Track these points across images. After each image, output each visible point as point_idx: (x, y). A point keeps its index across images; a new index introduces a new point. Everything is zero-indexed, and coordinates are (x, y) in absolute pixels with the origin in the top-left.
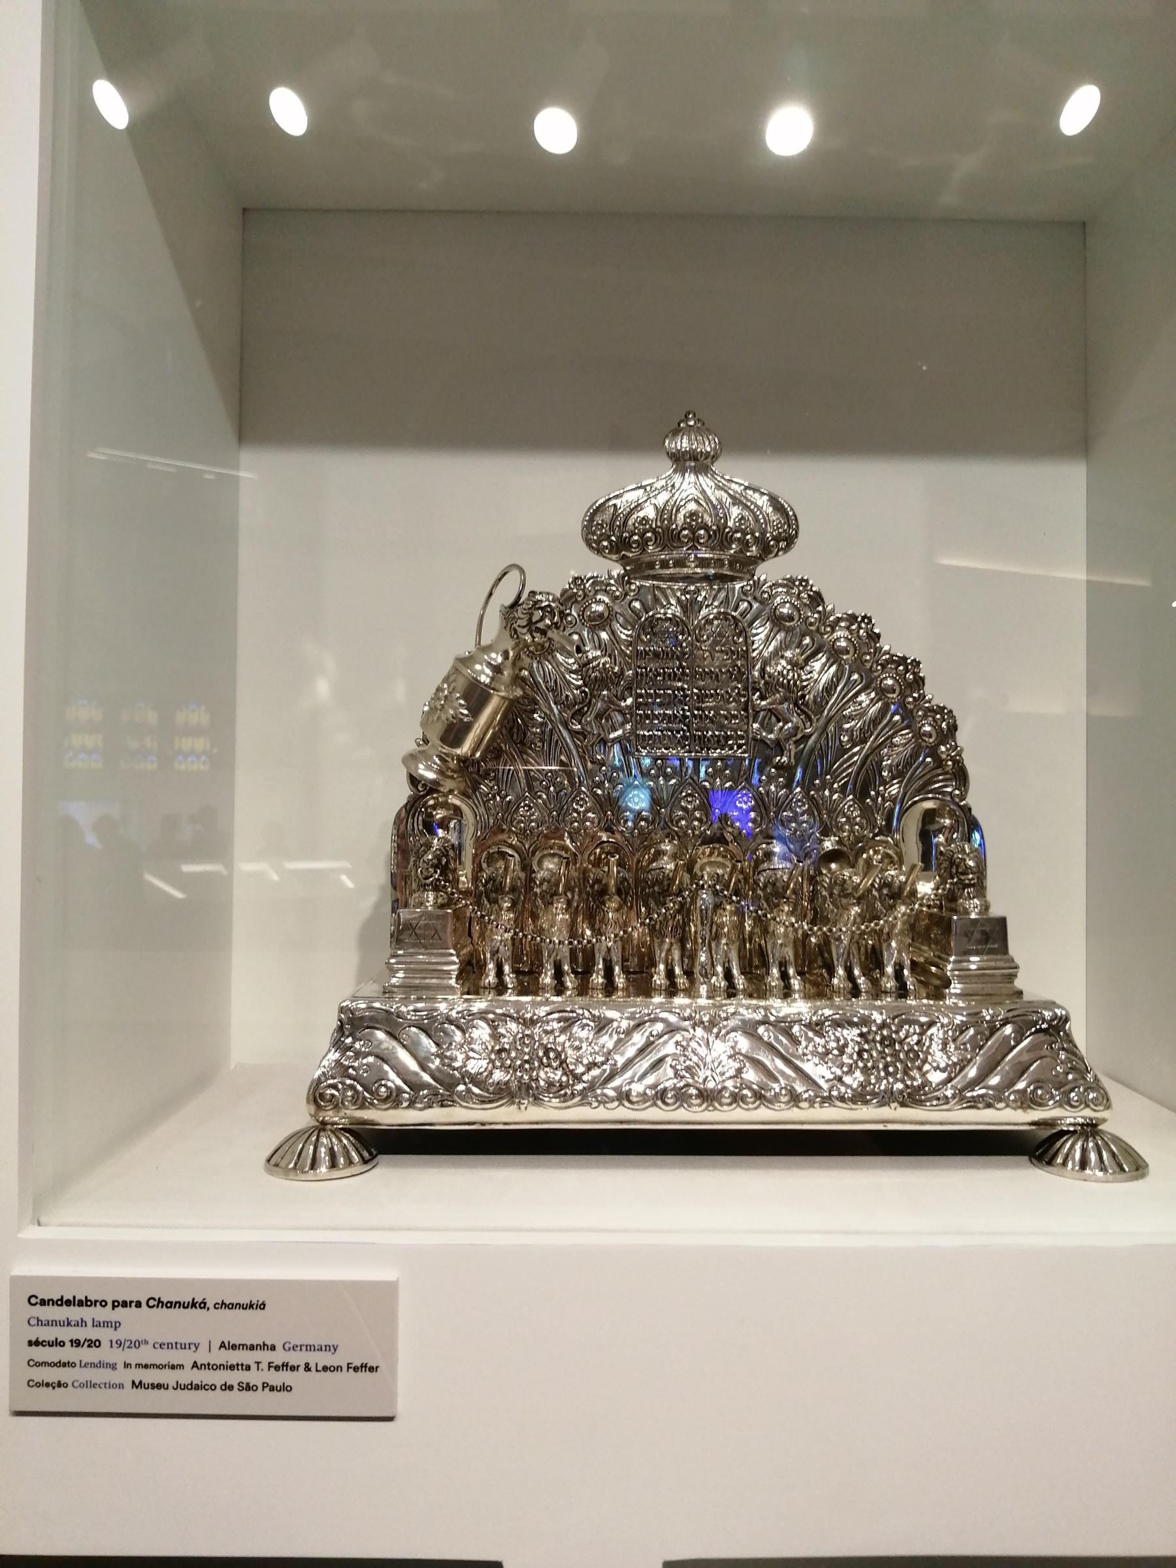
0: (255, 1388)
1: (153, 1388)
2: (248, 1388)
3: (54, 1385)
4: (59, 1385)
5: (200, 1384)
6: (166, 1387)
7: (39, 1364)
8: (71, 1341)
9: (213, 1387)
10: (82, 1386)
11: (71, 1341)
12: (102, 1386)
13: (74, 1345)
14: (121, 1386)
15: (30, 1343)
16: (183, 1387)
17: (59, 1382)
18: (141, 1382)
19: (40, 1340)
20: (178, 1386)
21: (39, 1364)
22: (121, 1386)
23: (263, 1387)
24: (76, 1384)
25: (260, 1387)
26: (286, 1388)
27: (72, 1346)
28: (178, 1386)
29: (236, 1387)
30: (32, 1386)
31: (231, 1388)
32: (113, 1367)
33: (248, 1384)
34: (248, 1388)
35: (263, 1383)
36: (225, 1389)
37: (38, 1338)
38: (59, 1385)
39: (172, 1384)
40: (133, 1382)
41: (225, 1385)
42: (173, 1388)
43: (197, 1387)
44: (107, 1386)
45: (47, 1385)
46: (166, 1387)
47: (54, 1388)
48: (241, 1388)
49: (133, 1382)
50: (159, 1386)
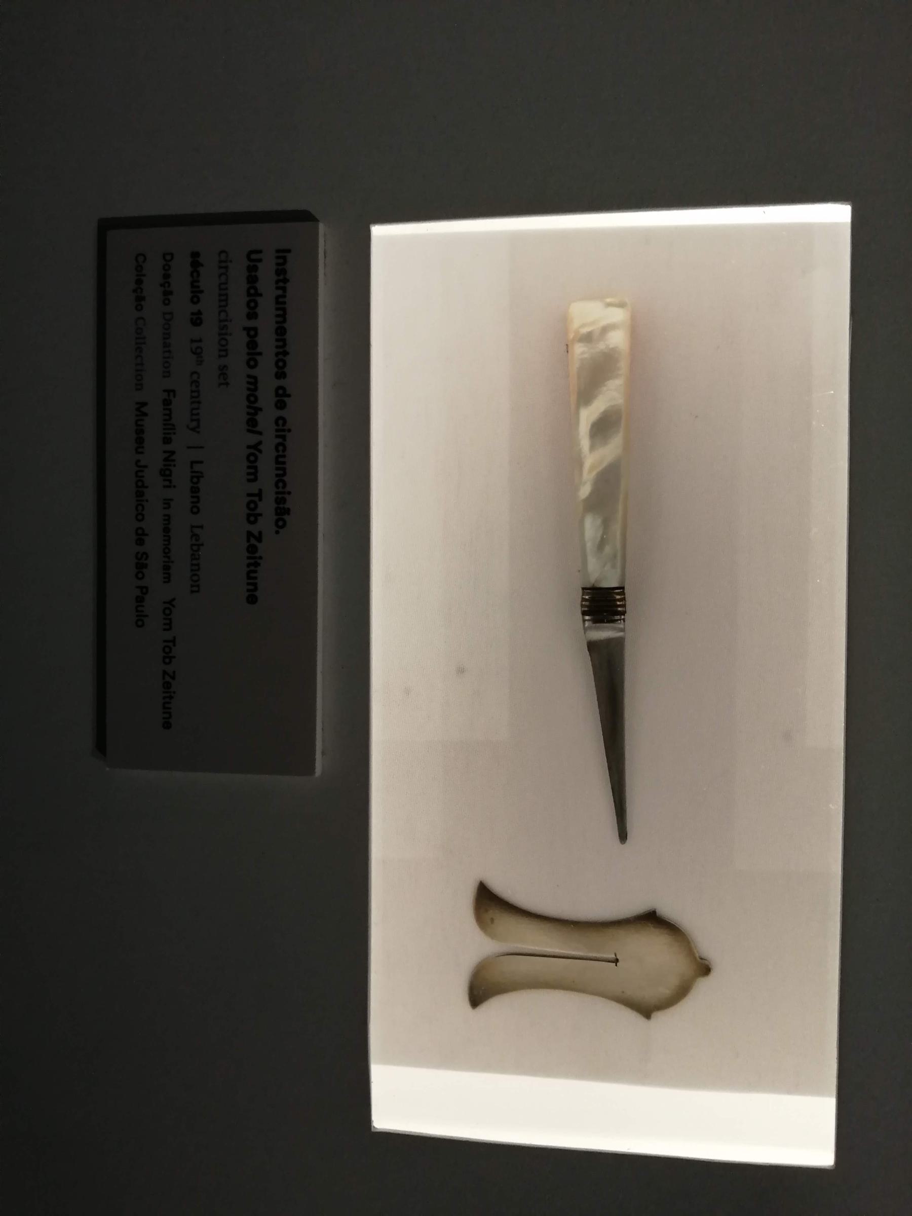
2: (141, 567)
3: (139, 290)
4: (140, 299)
6: (140, 450)
7: (167, 268)
8: (200, 313)
9: (140, 517)
11: (200, 313)
13: (194, 317)
15: (195, 255)
16: (140, 474)
17: (143, 299)
18: (146, 414)
19: (201, 269)
20: (140, 468)
21: (167, 268)
22: (139, 387)
23: (141, 588)
26: (140, 621)
27: (193, 314)
28: (140, 468)
30: (137, 260)
31: (140, 542)
32: (167, 374)
33: (146, 566)
34: (141, 567)
35: (146, 588)
36: (137, 534)
37: (202, 265)
40: (144, 404)
41: (144, 534)
43: (140, 494)
45: (139, 282)
46: (140, 450)
47: (135, 291)
48: (139, 556)
49: (144, 404)
50: (140, 441)
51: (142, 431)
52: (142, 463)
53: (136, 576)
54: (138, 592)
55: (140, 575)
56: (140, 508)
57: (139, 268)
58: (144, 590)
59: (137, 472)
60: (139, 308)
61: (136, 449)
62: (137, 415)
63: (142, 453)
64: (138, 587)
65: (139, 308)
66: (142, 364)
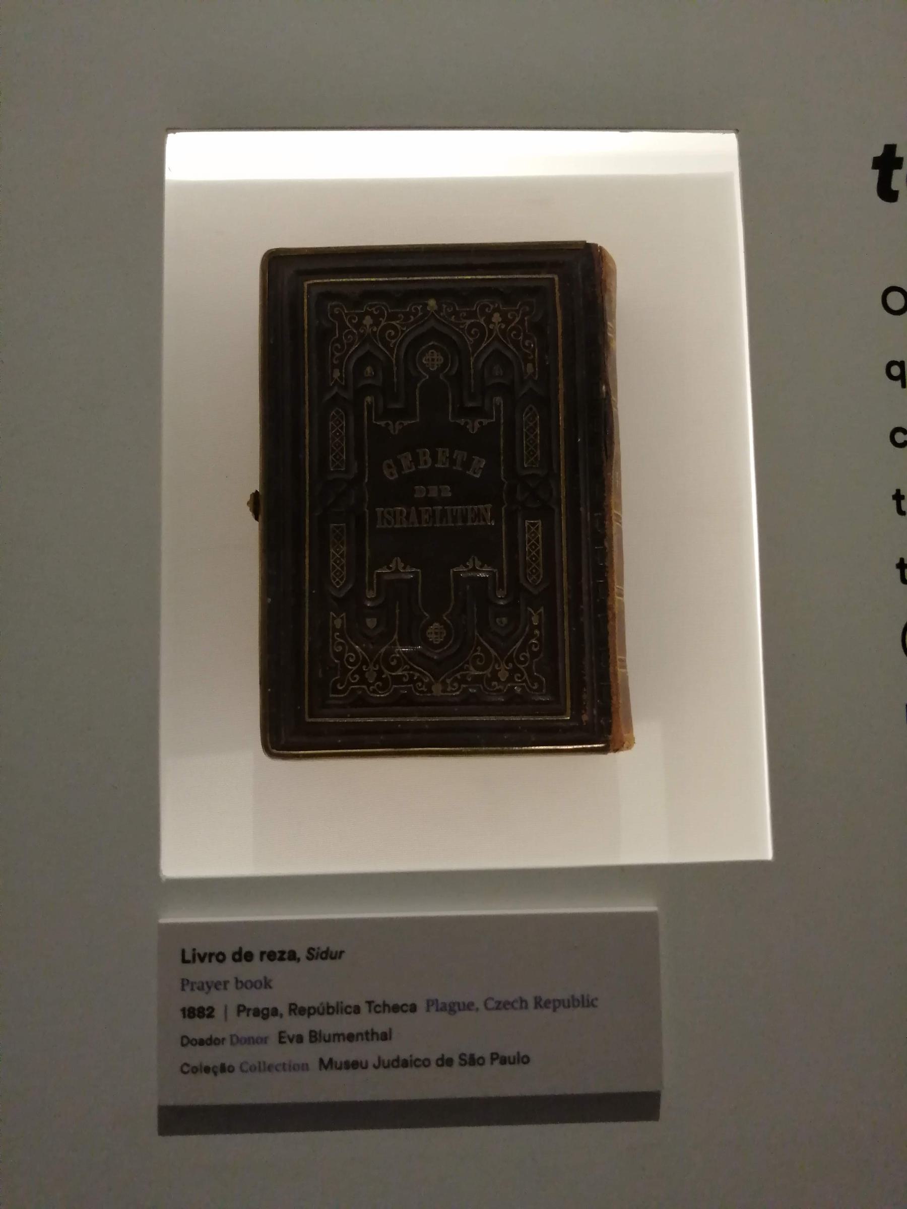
0: (481, 1061)
1: (347, 1068)
4: (223, 1068)
5: (409, 1059)
10: (253, 1069)
12: (280, 1068)
14: (305, 1067)
20: (381, 1064)
22: (305, 1067)
23: (493, 1060)
24: (245, 1068)
25: (488, 1060)
28: (381, 1064)
29: (456, 1060)
31: (449, 1062)
33: (472, 1056)
36: (442, 1065)
38: (223, 1068)
39: (373, 1060)
40: (321, 1061)
43: (405, 1064)
44: (287, 1067)
45: (207, 1070)
46: (364, 1065)
47: (215, 1074)
48: (463, 1062)
49: (321, 1061)
50: (355, 1065)
51: (347, 1063)
52: (377, 1064)
53: (482, 1065)
54: (497, 1062)
55: (525, 1060)
56: (418, 1063)
57: (195, 1070)
58: (495, 1056)
60: (231, 1069)
61: (363, 1068)
62: (332, 1067)
63: (367, 1062)
64: (492, 1063)
65: (231, 1069)
66: (284, 1064)
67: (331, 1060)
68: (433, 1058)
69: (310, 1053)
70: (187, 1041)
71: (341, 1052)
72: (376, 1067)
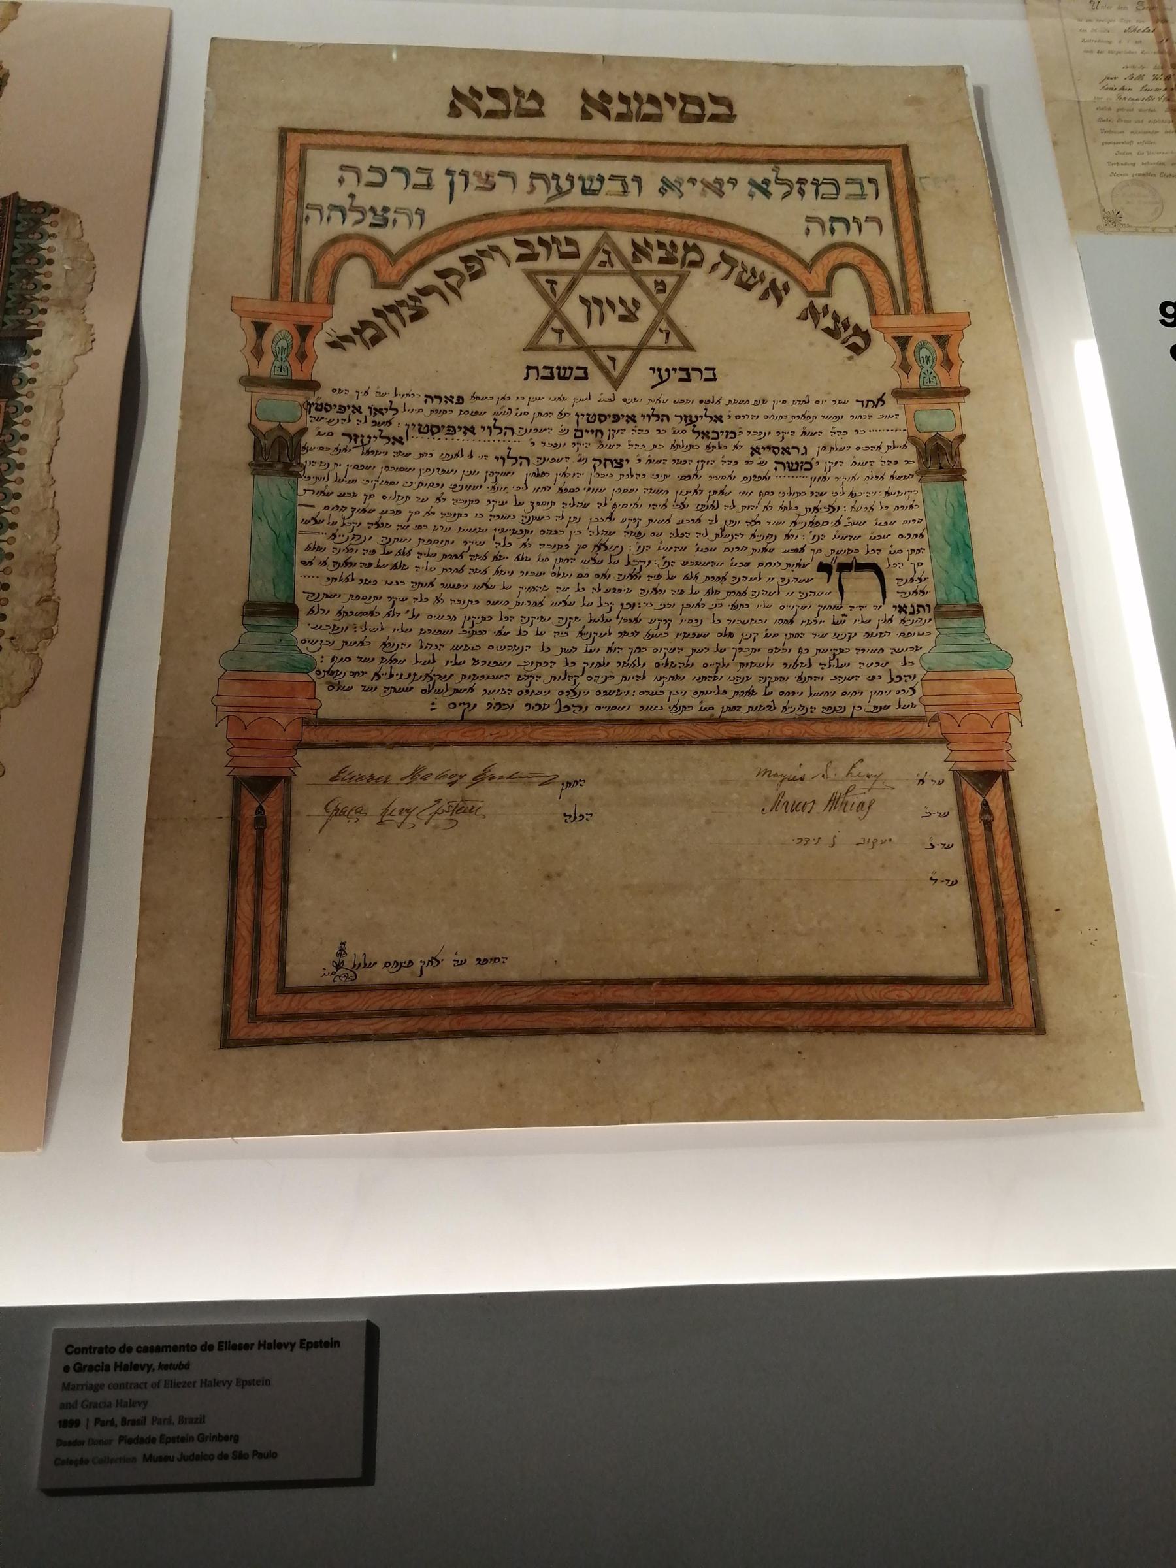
1: (160, 1461)
9: (210, 1457)
10: (102, 1462)
20: (184, 1458)
22: (134, 1460)
28: (184, 1458)
39: (178, 1455)
40: (145, 1455)
42: (178, 1460)
49: (145, 1455)
54: (256, 1457)
59: (185, 1460)
63: (173, 1457)
67: (151, 1455)
68: (216, 1454)
69: (138, 1451)
70: (60, 1443)
71: (157, 1449)
72: (179, 1460)
